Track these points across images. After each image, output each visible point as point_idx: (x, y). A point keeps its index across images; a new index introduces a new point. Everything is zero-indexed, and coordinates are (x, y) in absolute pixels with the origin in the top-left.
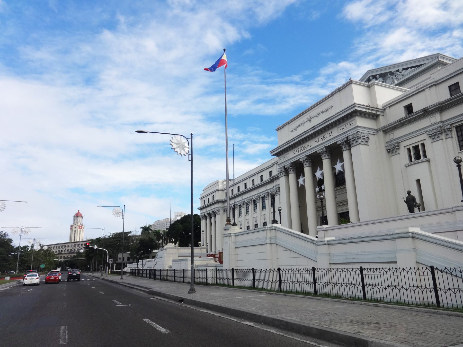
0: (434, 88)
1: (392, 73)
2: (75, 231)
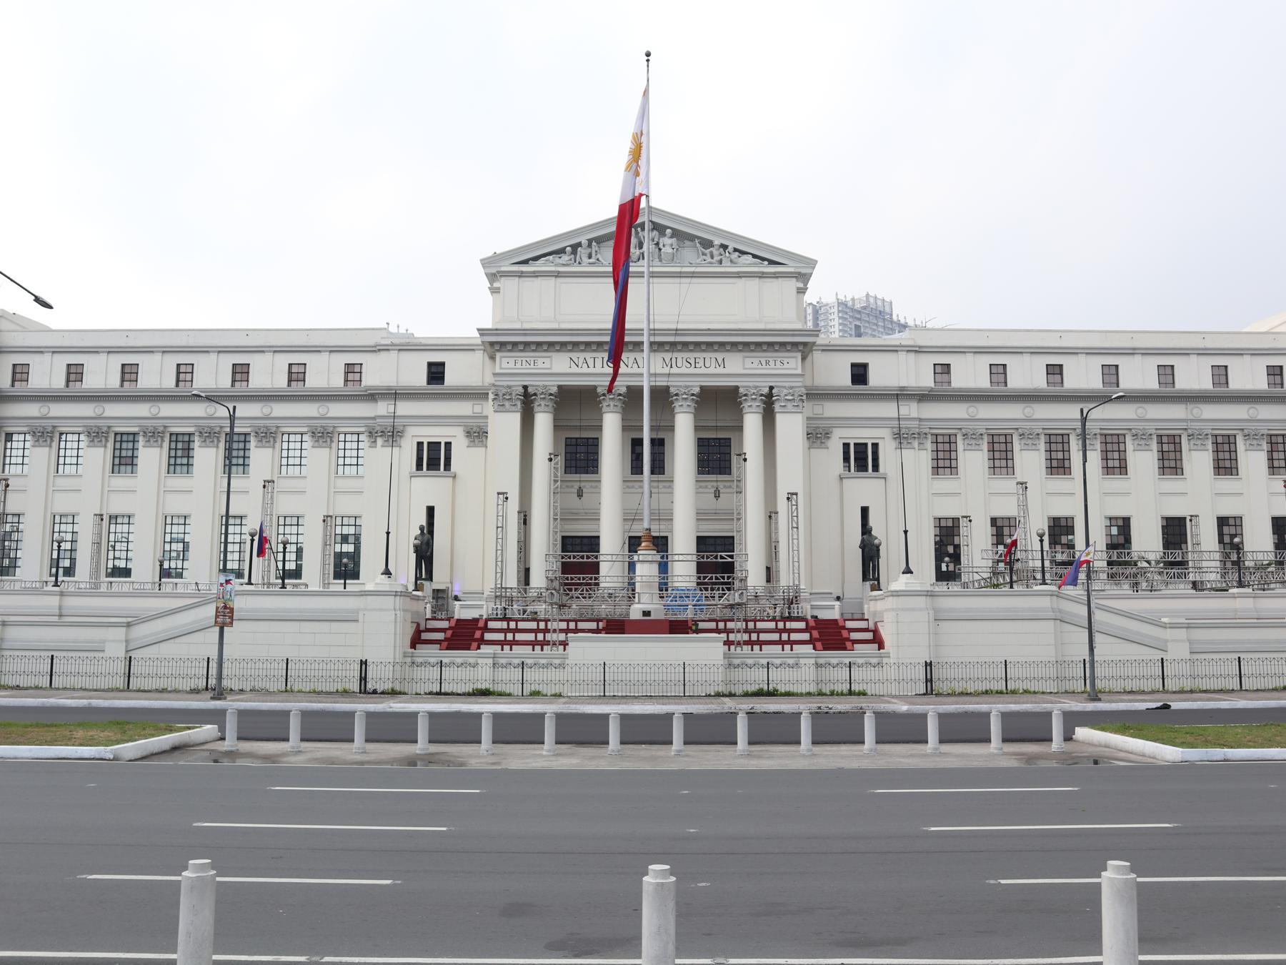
0: (912, 355)
1: (707, 244)
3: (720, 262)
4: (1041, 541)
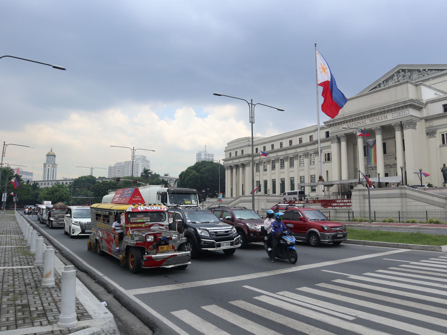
1: (419, 71)
2: (49, 169)
3: (424, 75)
4: (402, 170)
